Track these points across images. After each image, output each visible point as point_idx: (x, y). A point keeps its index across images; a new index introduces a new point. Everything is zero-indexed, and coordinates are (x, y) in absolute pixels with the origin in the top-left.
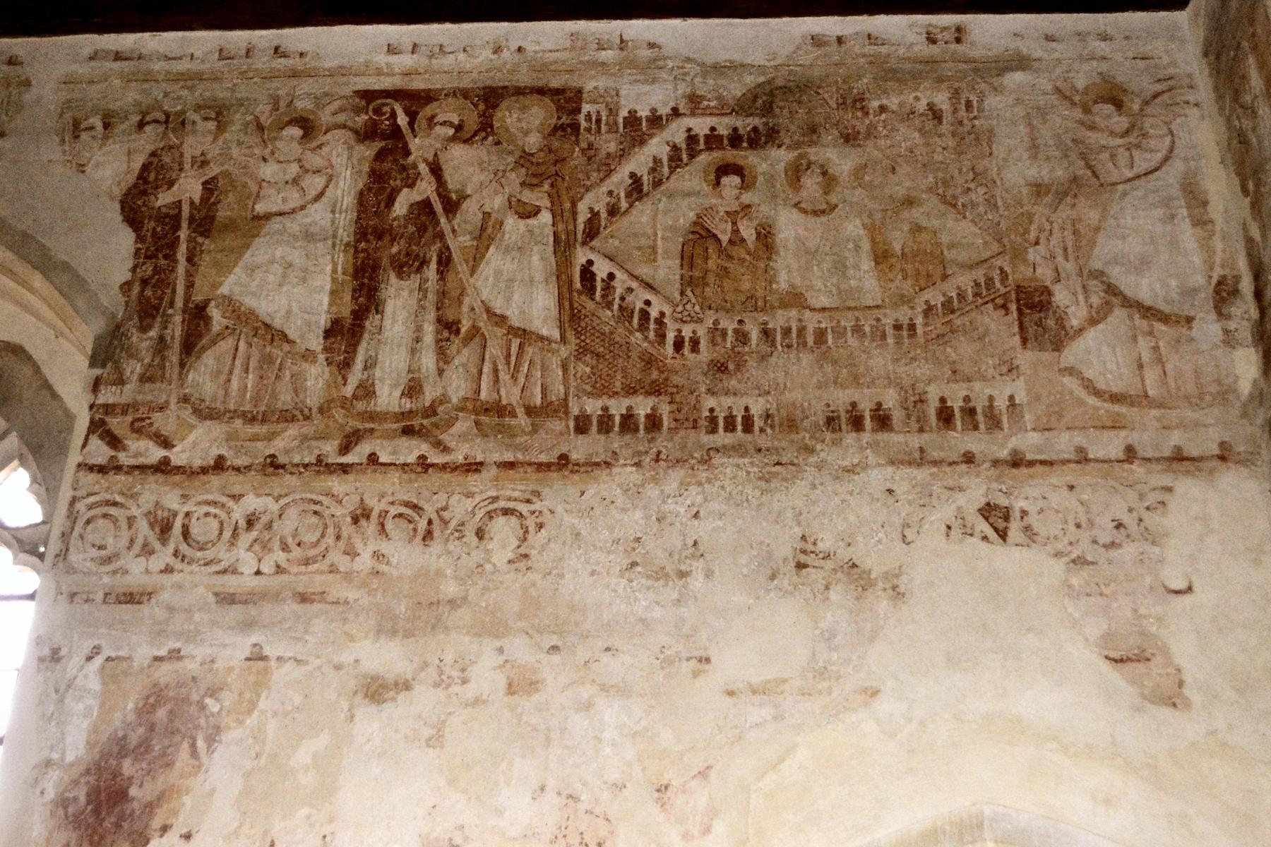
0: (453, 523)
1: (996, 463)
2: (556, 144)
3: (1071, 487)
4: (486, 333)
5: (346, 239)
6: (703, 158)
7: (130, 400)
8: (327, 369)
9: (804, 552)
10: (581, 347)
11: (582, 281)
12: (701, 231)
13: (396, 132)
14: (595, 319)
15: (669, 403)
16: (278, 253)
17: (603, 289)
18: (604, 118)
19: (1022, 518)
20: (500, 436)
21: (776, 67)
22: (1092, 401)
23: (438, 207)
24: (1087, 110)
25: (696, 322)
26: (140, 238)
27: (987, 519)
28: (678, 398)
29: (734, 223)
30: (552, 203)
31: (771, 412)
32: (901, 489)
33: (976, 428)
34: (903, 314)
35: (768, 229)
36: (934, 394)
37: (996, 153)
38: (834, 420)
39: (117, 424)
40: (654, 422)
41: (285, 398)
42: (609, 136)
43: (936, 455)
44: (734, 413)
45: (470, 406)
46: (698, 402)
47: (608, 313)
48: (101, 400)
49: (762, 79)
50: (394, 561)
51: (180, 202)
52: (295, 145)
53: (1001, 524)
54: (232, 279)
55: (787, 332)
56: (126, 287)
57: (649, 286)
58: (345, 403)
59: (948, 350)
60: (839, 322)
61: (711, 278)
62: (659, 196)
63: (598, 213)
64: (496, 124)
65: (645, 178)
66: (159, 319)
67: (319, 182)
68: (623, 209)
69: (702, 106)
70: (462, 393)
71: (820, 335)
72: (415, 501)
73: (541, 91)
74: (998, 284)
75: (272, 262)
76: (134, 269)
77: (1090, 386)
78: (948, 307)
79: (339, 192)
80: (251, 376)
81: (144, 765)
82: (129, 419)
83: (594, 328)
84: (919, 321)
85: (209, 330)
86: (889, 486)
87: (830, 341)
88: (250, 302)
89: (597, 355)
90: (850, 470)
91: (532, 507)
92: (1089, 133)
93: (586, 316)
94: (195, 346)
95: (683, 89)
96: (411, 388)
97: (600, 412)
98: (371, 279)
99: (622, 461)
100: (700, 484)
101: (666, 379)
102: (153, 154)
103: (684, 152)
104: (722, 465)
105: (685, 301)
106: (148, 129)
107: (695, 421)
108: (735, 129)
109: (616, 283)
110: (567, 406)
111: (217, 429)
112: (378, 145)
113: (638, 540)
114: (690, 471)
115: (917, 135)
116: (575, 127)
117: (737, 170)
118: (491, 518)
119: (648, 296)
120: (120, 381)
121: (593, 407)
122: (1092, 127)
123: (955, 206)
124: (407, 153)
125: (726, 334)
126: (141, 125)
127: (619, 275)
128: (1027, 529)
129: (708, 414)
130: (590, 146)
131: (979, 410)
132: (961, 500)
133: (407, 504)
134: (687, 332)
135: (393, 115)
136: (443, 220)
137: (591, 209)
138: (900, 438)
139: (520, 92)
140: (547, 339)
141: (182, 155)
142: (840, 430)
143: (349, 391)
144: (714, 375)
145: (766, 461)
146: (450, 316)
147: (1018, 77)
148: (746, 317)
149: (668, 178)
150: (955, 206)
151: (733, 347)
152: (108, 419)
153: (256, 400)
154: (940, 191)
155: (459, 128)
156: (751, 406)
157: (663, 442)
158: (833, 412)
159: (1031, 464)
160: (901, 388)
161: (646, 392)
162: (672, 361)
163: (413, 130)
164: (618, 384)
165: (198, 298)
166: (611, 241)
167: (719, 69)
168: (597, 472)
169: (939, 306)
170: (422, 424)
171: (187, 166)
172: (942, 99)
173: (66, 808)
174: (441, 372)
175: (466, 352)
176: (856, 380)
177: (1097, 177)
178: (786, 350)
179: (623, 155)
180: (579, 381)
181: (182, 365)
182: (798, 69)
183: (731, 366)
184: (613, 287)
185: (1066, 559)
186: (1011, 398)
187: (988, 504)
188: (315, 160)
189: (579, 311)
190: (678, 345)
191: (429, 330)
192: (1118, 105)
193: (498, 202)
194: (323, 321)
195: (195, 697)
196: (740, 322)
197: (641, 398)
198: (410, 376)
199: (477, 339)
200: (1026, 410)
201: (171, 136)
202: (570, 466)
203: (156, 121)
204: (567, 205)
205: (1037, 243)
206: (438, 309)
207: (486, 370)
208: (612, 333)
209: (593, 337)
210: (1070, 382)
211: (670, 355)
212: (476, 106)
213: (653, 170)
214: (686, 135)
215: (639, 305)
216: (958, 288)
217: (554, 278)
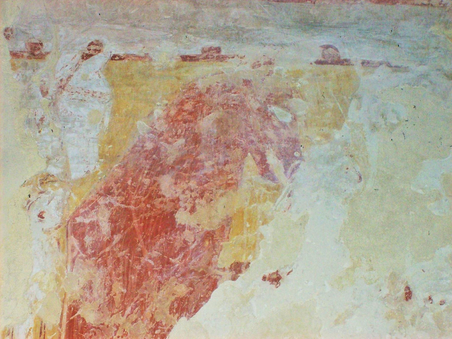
81: (193, 184)
173: (80, 236)
195: (254, 105)
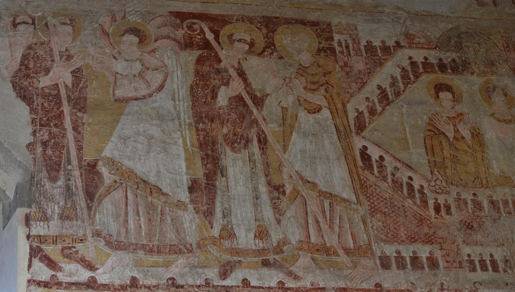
2: (322, 61)
4: (304, 195)
5: (188, 121)
6: (424, 77)
7: (56, 234)
8: (196, 216)
10: (372, 208)
11: (362, 161)
12: (433, 130)
13: (206, 45)
15: (440, 249)
16: (141, 129)
17: (378, 167)
18: (351, 45)
20: (332, 269)
23: (249, 102)
26: (33, 111)
28: (445, 246)
29: (455, 126)
30: (328, 103)
31: (507, 258)
35: (477, 130)
39: (49, 249)
40: (433, 263)
41: (171, 236)
44: (484, 258)
46: (459, 249)
47: (386, 184)
48: (34, 232)
49: (450, 26)
51: (57, 85)
52: (135, 48)
54: (110, 146)
56: (31, 147)
57: (410, 167)
58: (214, 241)
61: (448, 163)
62: (400, 103)
63: (362, 113)
64: (277, 45)
65: (388, 90)
66: (62, 172)
67: (159, 77)
70: (297, 238)
73: (303, 23)
75: (138, 134)
76: (34, 133)
79: (175, 86)
80: (142, 219)
82: (59, 247)
83: (378, 194)
85: (102, 182)
88: (128, 163)
89: (384, 214)
93: (371, 186)
94: (95, 195)
96: (260, 233)
97: (395, 255)
101: (435, 233)
102: (29, 48)
103: (410, 73)
105: (435, 179)
106: (20, 27)
108: (440, 60)
109: (385, 163)
110: (371, 249)
111: (127, 258)
116: (333, 51)
117: (449, 89)
119: (410, 174)
120: (45, 218)
121: (390, 250)
124: (219, 61)
125: (467, 203)
126: (15, 25)
127: (385, 156)
129: (467, 258)
130: (346, 65)
134: (441, 200)
135: (202, 32)
136: (255, 111)
137: (357, 110)
139: (288, 22)
140: (348, 201)
141: (51, 50)
143: (216, 232)
144: (465, 231)
146: (276, 181)
148: (479, 191)
149: (403, 91)
151: (474, 212)
152: (43, 247)
153: (150, 236)
161: (423, 241)
162: (436, 220)
163: (219, 43)
164: (402, 234)
165: (88, 158)
166: (376, 133)
170: (275, 259)
171: (57, 58)
174: (279, 222)
175: (293, 207)
178: (508, 215)
179: (370, 73)
180: (376, 232)
181: (89, 208)
182: (472, 20)
183: (475, 226)
184: (385, 166)
188: (152, 61)
189: (365, 182)
190: (437, 209)
191: (263, 189)
193: (291, 99)
194: (185, 180)
196: (474, 194)
197: (420, 245)
198: (258, 223)
199: (298, 199)
201: (40, 34)
203: (24, 23)
204: (340, 106)
206: (266, 176)
207: (310, 221)
209: (378, 201)
211: (433, 216)
212: (260, 29)
213: (392, 85)
215: (405, 180)
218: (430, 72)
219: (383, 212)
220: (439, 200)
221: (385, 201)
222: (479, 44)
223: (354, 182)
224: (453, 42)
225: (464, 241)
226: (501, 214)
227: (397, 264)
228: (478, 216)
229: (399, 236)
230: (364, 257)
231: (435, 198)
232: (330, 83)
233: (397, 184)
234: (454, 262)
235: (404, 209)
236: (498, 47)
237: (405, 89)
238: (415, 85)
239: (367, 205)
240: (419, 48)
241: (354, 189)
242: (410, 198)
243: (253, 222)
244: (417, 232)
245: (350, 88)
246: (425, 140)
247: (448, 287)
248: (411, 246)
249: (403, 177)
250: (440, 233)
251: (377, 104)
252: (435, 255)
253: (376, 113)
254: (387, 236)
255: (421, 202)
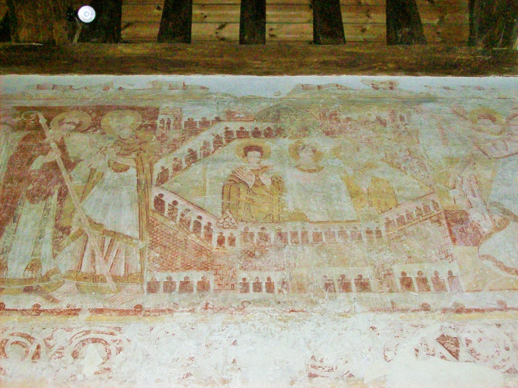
0: (55, 348)
1: (444, 310)
3: (499, 325)
4: (88, 234)
9: (314, 367)
10: (153, 242)
11: (155, 205)
13: (38, 127)
14: (163, 226)
17: (169, 210)
18: (172, 122)
19: (467, 344)
20: (94, 293)
21: (281, 99)
22: (504, 274)
23: (61, 165)
24: (474, 122)
25: (232, 228)
27: (443, 345)
28: (220, 272)
29: (257, 176)
30: (137, 164)
31: (285, 281)
32: (380, 328)
33: (428, 290)
34: (372, 225)
36: (397, 270)
37: (421, 142)
38: (330, 285)
40: (203, 286)
42: (175, 131)
43: (403, 305)
44: (260, 281)
45: (73, 275)
46: (235, 274)
47: (173, 223)
49: (272, 105)
50: (9, 372)
53: (453, 348)
55: (295, 234)
59: (404, 245)
60: (329, 229)
63: (167, 170)
64: (103, 124)
68: (183, 168)
69: (235, 117)
70: (68, 268)
71: (317, 237)
72: (29, 334)
73: (133, 109)
74: (432, 209)
77: (500, 265)
78: (401, 220)
83: (162, 231)
84: (383, 229)
86: (372, 324)
87: (324, 240)
89: (165, 247)
90: (344, 315)
91: (115, 338)
92: (478, 133)
93: (157, 225)
95: (222, 109)
98: (12, 203)
99: (180, 309)
100: (237, 323)
103: (223, 139)
104: (253, 311)
105: (225, 217)
107: (233, 285)
109: (178, 207)
110: (142, 276)
112: (25, 133)
113: (192, 359)
114: (229, 315)
115: (371, 132)
116: (154, 127)
117: (258, 149)
118: (84, 344)
121: (161, 277)
122: (480, 130)
123: (399, 168)
124: (45, 137)
127: (180, 202)
128: (472, 351)
129: (242, 281)
130: (163, 135)
131: (429, 279)
132: (423, 333)
133: (22, 335)
134: (226, 234)
135: (37, 118)
137: (163, 168)
138: (377, 296)
140: (130, 237)
142: (335, 291)
145: (284, 309)
146: (64, 223)
147: (430, 105)
148: (267, 226)
150: (399, 168)
151: (258, 243)
154: (389, 160)
155: (79, 125)
156: (272, 277)
157: (209, 297)
158: (329, 280)
159: (469, 311)
160: (375, 267)
162: (216, 251)
163: (48, 125)
164: (178, 263)
167: (246, 100)
168: (163, 316)
169: (395, 221)
172: (385, 115)
174: (55, 256)
175: (73, 244)
176: (344, 262)
177: (487, 155)
178: (294, 244)
180: (151, 262)
182: (294, 100)
183: (257, 254)
184: (176, 209)
185: (503, 370)
186: (450, 273)
187: (443, 336)
190: (221, 242)
191: (49, 231)
192: (493, 120)
196: (263, 228)
197: (195, 272)
198: (33, 258)
199: (81, 237)
200: (461, 280)
202: (143, 312)
204: (147, 166)
205: (454, 188)
206: (56, 220)
207: (86, 254)
208: (175, 234)
209: (161, 237)
210: (489, 263)
211: (215, 247)
214: (225, 131)
215: (194, 218)
216: (407, 211)
217: (136, 204)
218: (243, 138)
219: (164, 245)
220: (224, 234)
221: (168, 237)
222: (296, 115)
223: (141, 222)
224: (271, 115)
225: (242, 267)
226: (287, 243)
227: (164, 288)
228: (262, 246)
229: (174, 265)
230: (132, 282)
231: (220, 233)
232: (143, 149)
233: (184, 223)
234: (227, 285)
235: (186, 242)
236: (314, 117)
237: (215, 150)
238: (225, 147)
239: (148, 240)
240: (237, 121)
241: (140, 227)
242: (195, 233)
243: (29, 256)
244: (194, 261)
245: (161, 152)
246: (223, 188)
247: (213, 306)
248: (184, 273)
249: (192, 217)
250: (218, 261)
251: (184, 163)
252: (208, 279)
253: (181, 169)
254: (161, 265)
255: (205, 236)
